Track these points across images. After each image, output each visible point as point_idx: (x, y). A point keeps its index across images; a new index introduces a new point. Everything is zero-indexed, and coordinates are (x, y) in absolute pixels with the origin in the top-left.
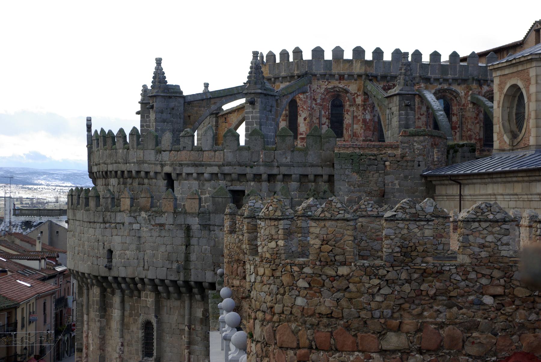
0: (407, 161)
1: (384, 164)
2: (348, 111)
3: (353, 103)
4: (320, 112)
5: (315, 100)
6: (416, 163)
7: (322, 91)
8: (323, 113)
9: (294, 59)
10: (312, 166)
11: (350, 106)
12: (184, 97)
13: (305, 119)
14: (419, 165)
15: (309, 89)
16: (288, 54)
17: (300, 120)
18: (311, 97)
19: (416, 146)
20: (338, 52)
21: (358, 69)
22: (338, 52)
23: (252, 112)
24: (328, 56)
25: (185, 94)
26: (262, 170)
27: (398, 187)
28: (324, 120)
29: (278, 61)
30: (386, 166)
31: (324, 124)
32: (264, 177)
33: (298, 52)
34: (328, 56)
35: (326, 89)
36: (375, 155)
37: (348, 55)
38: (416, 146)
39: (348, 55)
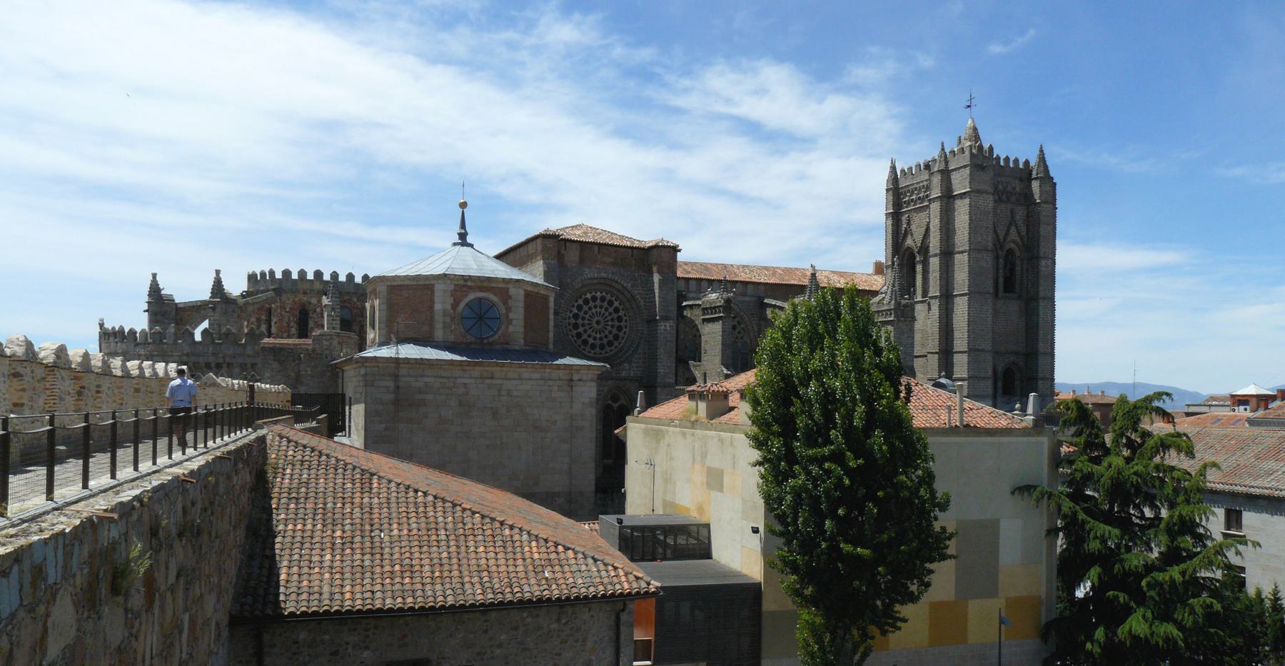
0: (317, 354)
1: (299, 356)
2: (312, 318)
3: (315, 311)
4: (289, 318)
5: (284, 308)
6: (324, 356)
7: (290, 302)
8: (292, 318)
9: (270, 277)
10: (249, 356)
11: (313, 314)
12: (176, 304)
13: (276, 323)
14: (327, 357)
15: (278, 300)
16: (265, 274)
17: (273, 324)
18: (281, 307)
19: (325, 343)
20: (302, 273)
21: (318, 286)
22: (302, 273)
23: (213, 316)
24: (295, 276)
25: (176, 301)
26: (211, 359)
27: (310, 373)
28: (292, 324)
29: (259, 278)
30: (300, 358)
31: (293, 327)
32: (213, 365)
33: (272, 273)
34: (295, 276)
35: (293, 301)
36: (291, 349)
37: (310, 276)
38: (325, 343)
39: (310, 276)
